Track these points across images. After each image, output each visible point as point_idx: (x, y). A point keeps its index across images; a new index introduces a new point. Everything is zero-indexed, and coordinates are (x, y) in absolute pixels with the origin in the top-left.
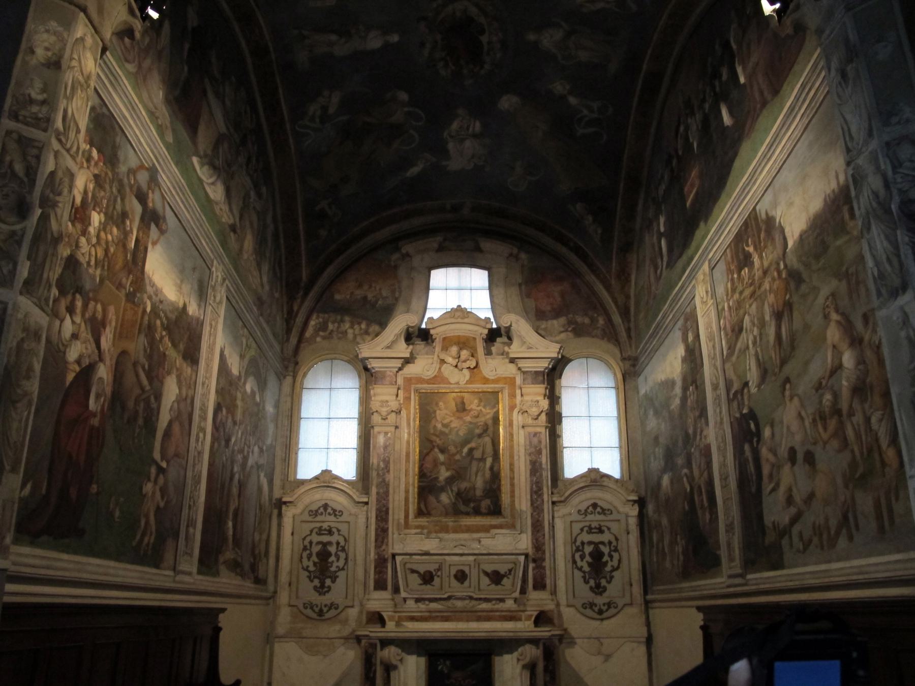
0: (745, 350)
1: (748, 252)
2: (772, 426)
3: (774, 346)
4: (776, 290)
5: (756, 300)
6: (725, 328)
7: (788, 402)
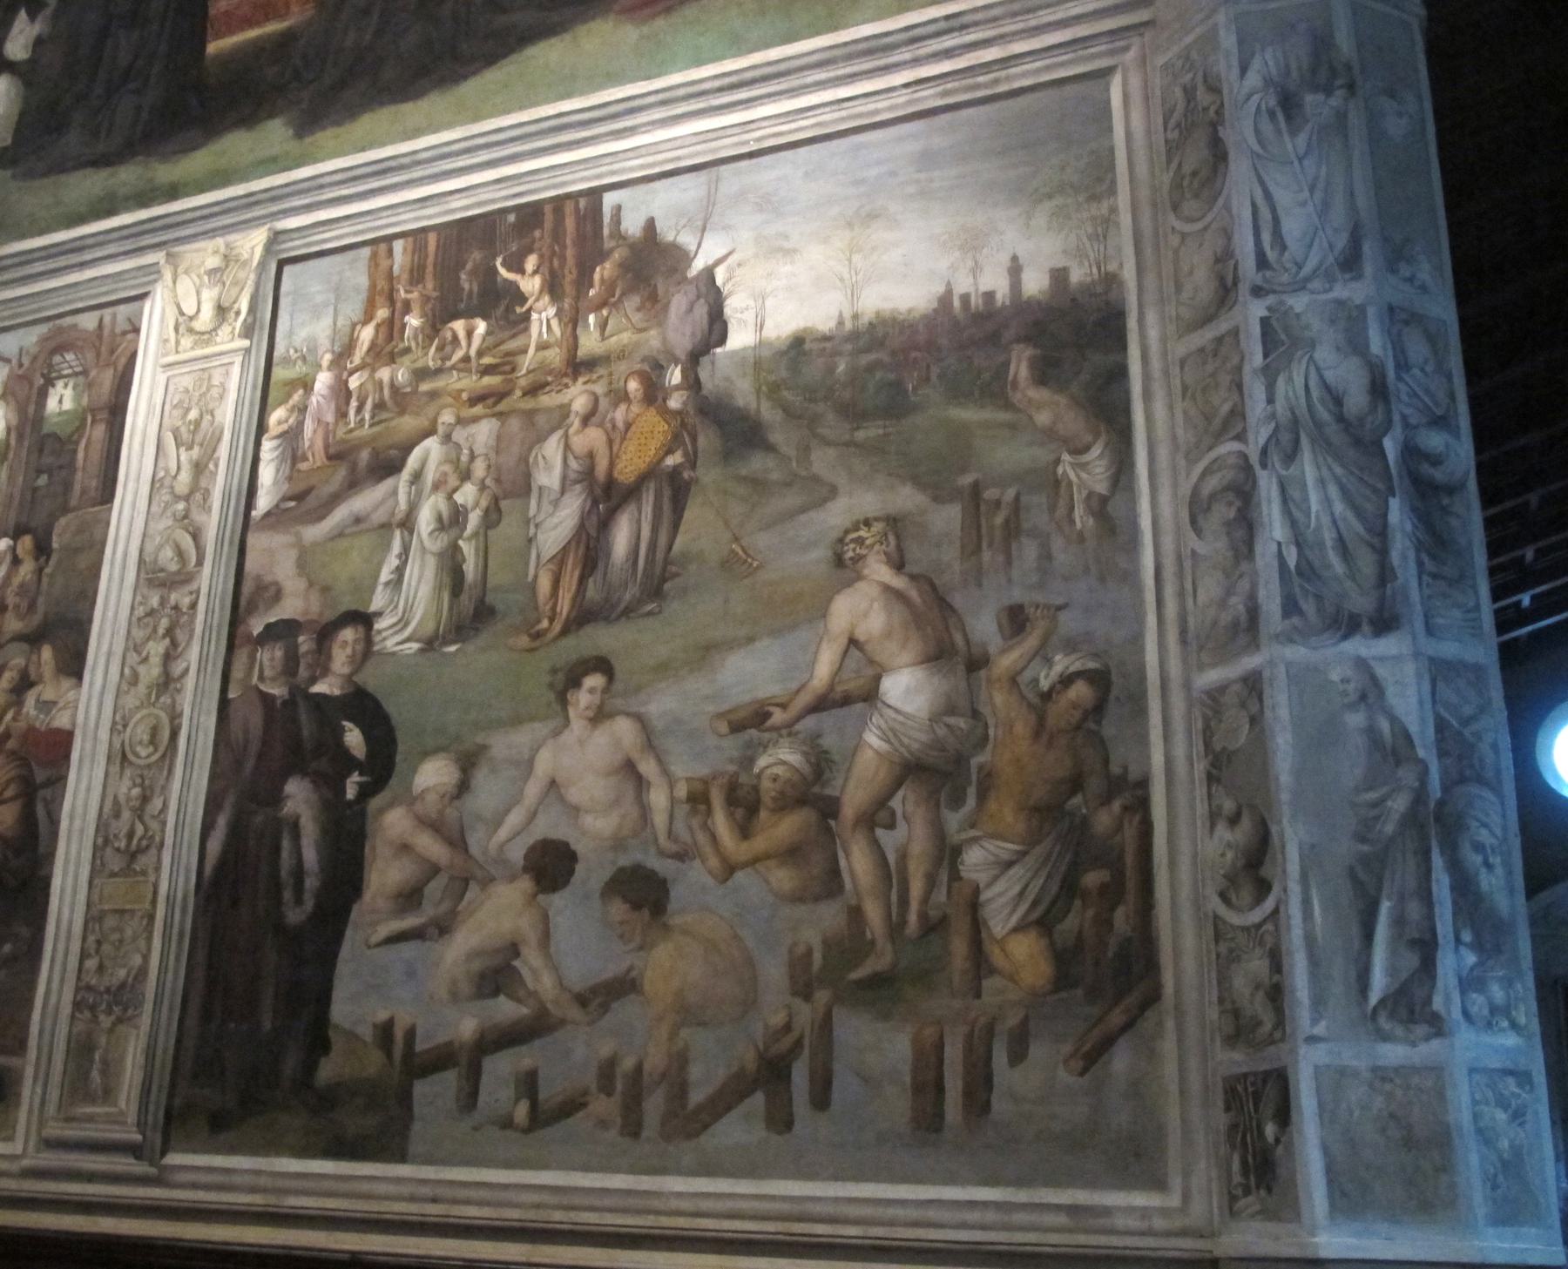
0: (386, 527)
1: (514, 287)
2: (468, 763)
3: (560, 559)
4: (620, 424)
5: (500, 415)
6: (291, 436)
7: (577, 725)
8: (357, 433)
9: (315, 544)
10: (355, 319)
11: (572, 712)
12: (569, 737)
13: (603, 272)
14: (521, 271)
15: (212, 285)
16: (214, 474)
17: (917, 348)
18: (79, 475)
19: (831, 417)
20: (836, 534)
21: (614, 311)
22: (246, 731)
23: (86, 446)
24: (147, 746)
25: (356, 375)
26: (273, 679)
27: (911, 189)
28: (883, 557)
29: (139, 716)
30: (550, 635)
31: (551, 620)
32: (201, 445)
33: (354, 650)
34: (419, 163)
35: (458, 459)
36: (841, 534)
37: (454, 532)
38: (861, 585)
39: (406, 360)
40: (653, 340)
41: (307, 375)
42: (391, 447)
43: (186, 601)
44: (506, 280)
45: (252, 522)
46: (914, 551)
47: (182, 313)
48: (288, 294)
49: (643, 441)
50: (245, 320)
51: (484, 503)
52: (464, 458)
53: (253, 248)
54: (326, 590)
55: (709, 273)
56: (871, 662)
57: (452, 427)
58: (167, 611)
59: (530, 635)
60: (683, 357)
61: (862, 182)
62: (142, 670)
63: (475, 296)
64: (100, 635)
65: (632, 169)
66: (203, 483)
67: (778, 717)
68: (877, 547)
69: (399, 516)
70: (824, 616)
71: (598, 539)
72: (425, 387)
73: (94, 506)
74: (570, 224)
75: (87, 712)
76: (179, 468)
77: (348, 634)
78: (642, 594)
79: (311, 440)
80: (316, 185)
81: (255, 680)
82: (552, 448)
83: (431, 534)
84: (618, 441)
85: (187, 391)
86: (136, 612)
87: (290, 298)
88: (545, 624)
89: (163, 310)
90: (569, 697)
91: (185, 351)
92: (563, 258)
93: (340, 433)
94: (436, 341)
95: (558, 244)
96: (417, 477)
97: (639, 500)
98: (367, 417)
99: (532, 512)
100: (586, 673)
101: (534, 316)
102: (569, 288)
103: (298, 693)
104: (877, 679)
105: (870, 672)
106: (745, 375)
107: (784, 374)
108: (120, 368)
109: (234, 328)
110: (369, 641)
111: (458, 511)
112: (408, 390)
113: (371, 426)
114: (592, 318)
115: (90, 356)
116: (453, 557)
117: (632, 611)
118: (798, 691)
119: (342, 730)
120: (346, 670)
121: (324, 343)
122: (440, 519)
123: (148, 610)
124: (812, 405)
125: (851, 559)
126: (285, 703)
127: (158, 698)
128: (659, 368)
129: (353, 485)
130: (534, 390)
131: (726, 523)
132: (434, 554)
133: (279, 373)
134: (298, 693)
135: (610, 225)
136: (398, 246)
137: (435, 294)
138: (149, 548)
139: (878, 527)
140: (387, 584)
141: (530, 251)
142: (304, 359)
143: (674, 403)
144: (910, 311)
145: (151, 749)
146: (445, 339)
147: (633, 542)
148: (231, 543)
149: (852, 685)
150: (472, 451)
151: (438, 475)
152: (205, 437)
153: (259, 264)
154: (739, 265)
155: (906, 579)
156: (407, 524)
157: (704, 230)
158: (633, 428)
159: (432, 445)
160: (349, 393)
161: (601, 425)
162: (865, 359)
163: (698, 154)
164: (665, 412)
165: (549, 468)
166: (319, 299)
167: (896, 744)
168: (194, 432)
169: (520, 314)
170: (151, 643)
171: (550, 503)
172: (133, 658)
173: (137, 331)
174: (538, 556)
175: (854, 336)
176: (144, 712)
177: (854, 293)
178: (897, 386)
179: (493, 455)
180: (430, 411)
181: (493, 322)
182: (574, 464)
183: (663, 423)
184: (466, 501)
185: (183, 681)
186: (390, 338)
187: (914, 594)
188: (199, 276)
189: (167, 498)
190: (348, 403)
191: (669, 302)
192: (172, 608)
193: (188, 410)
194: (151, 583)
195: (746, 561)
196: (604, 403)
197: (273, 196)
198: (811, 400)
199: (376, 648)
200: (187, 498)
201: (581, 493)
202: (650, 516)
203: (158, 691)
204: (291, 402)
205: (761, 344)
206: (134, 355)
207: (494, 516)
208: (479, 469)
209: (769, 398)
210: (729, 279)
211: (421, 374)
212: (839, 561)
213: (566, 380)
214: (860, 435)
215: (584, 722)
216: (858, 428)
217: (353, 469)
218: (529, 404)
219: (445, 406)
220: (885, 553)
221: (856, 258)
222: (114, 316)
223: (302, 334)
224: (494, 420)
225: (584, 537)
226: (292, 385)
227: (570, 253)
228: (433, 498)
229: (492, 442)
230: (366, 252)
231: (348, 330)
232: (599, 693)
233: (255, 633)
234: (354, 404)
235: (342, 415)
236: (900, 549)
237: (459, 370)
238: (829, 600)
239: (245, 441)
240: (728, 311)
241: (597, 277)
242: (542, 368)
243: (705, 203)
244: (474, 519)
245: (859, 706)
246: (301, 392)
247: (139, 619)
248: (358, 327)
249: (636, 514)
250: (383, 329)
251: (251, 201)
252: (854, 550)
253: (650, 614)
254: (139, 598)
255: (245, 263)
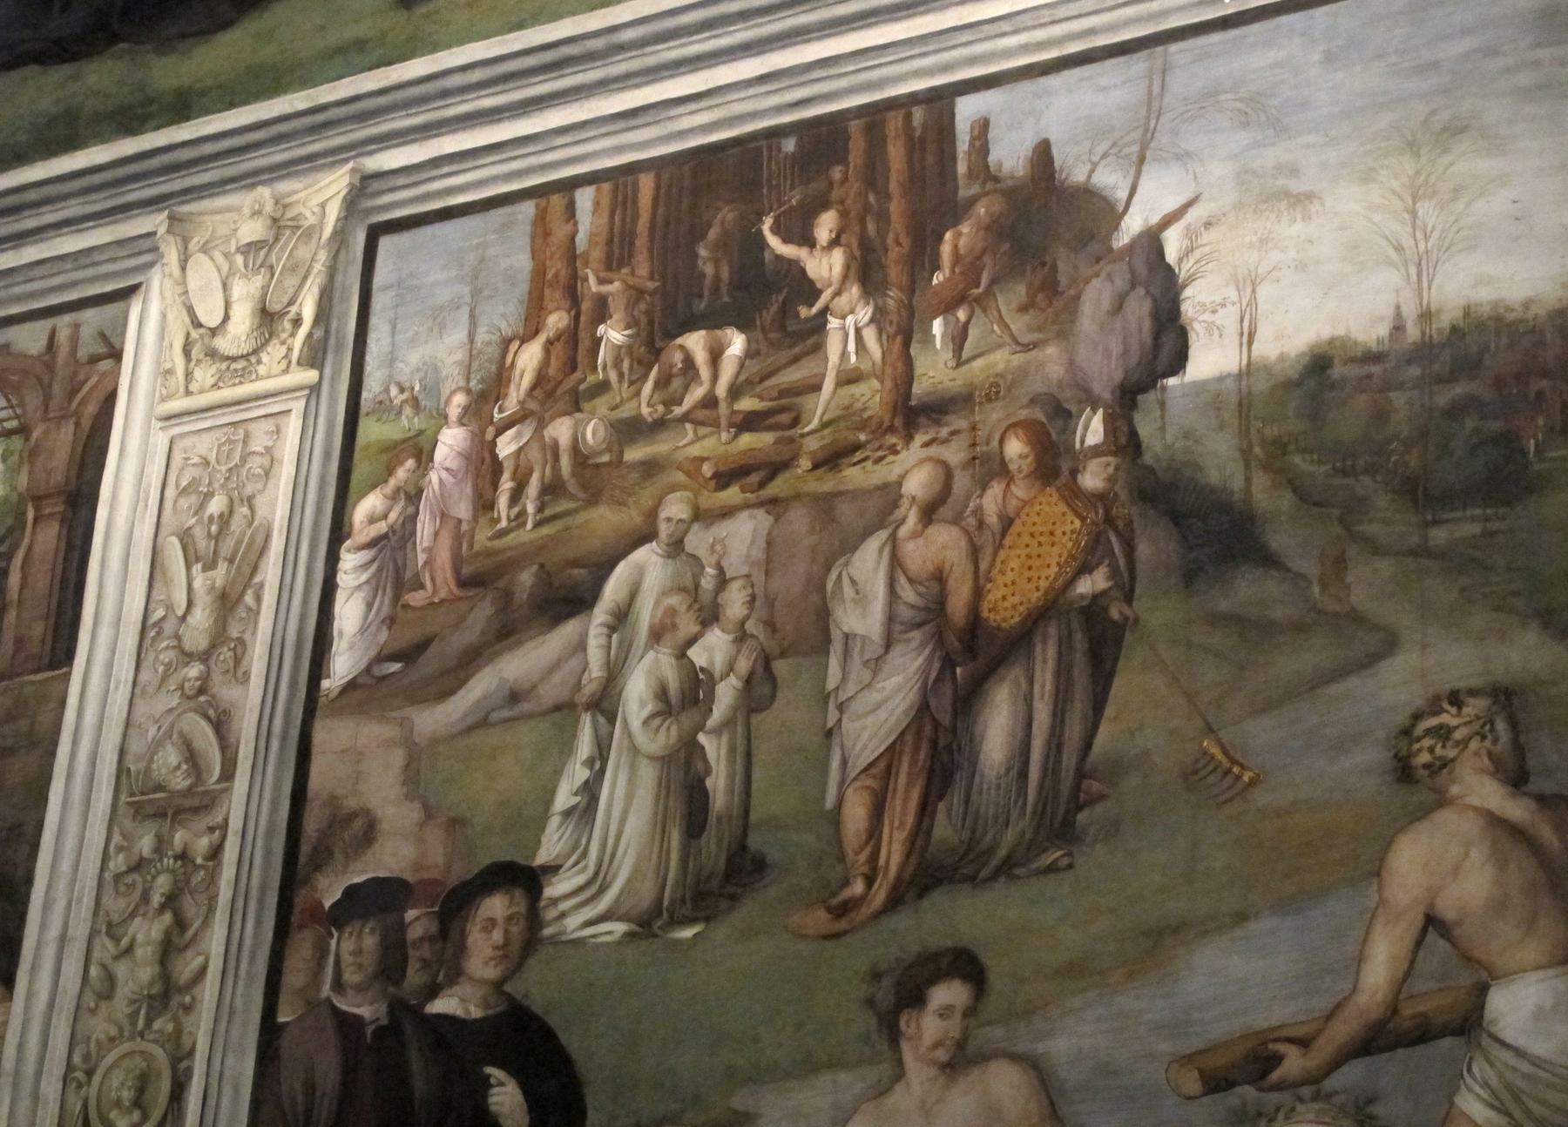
0: (565, 709)
1: (795, 270)
4: (992, 519)
5: (774, 505)
7: (918, 1074)
8: (509, 539)
9: (435, 741)
10: (508, 331)
11: (907, 1049)
12: (900, 1099)
13: (957, 240)
14: (809, 241)
15: (251, 270)
16: (255, 613)
17: (1545, 374)
18: (11, 616)
19: (1382, 501)
20: (1402, 719)
21: (978, 311)
22: (310, 1087)
23: (24, 562)
24: (129, 1112)
25: (511, 433)
26: (360, 988)
27: (1524, 79)
28: (1486, 761)
29: (110, 1059)
30: (866, 911)
31: (870, 881)
32: (231, 561)
33: (506, 932)
34: (622, 48)
35: (697, 586)
36: (1407, 723)
37: (688, 719)
38: (1446, 816)
39: (602, 404)
40: (1052, 362)
41: (421, 432)
42: (576, 563)
43: (203, 843)
44: (779, 258)
45: (322, 700)
46: (1545, 751)
47: (197, 324)
48: (385, 288)
49: (1034, 550)
50: (310, 335)
51: (744, 665)
52: (708, 582)
53: (323, 205)
54: (456, 824)
55: (1152, 240)
56: (1468, 960)
57: (685, 526)
58: (169, 862)
59: (829, 910)
60: (1107, 395)
61: (1435, 65)
62: (121, 970)
63: (724, 289)
64: (47, 906)
65: (1007, 53)
66: (234, 632)
67: (1294, 1063)
68: (1474, 744)
69: (589, 689)
70: (1378, 874)
71: (954, 730)
72: (633, 454)
73: (38, 671)
74: (896, 153)
75: (21, 1047)
76: (190, 604)
77: (496, 906)
78: (1037, 829)
79: (429, 550)
80: (435, 89)
81: (326, 990)
82: (868, 563)
83: (646, 722)
84: (988, 551)
85: (207, 463)
86: (112, 865)
87: (391, 293)
88: (858, 887)
89: (164, 316)
90: (902, 1024)
91: (201, 392)
92: (883, 217)
93: (482, 537)
94: (656, 369)
95: (876, 192)
96: (622, 617)
97: (1030, 656)
98: (530, 508)
99: (832, 683)
100: (933, 980)
101: (833, 323)
102: (895, 273)
103: (405, 1012)
104: (1482, 990)
105: (1466, 979)
106: (1222, 427)
107: (1294, 425)
108: (86, 423)
109: (290, 349)
110: (534, 919)
111: (698, 681)
112: (605, 458)
113: (538, 525)
114: (937, 326)
115: (33, 400)
116: (688, 764)
117: (1018, 865)
118: (1329, 1017)
119: (486, 1083)
120: (491, 973)
121: (452, 376)
122: (662, 694)
123: (135, 858)
124: (1350, 481)
125: (1426, 766)
126: (381, 1033)
127: (149, 1022)
128: (1063, 414)
129: (506, 633)
130: (832, 459)
131: (1190, 697)
132: (652, 758)
133: (371, 431)
134: (405, 1012)
135: (969, 153)
136: (585, 198)
137: (651, 285)
138: (136, 746)
139: (1475, 707)
140: (567, 814)
141: (825, 206)
142: (415, 403)
143: (1092, 479)
144: (1527, 305)
145: (136, 1115)
146: (671, 366)
147: (1020, 736)
148: (284, 738)
149: (1430, 1001)
150: (720, 569)
151: (659, 614)
152: (239, 542)
153: (335, 233)
154: (1208, 225)
155: (1533, 805)
156: (605, 703)
157: (1142, 160)
158: (1016, 527)
159: (648, 562)
160: (497, 467)
161: (956, 521)
162: (1444, 397)
163: (1126, 23)
164: (1073, 493)
165: (861, 598)
166: (444, 296)
167: (1518, 1114)
168: (217, 538)
169: (808, 320)
170: (138, 920)
171: (866, 663)
172: (105, 948)
173: (117, 355)
174: (844, 763)
175: (1424, 351)
176: (125, 1047)
177: (1422, 268)
178: (1508, 442)
179: (759, 578)
180: (646, 497)
181: (758, 334)
182: (908, 593)
183: (1070, 516)
184: (712, 663)
185: (196, 990)
186: (571, 365)
187: (1547, 835)
188: (226, 255)
189: (168, 656)
190: (495, 485)
191: (1077, 298)
192: (176, 858)
193: (209, 495)
194: (138, 810)
195: (1228, 772)
196: (961, 482)
197: (360, 111)
198: (1344, 473)
199: (548, 932)
200: (205, 657)
201: (923, 645)
202: (1049, 687)
203: (150, 1007)
204: (393, 482)
205: (1249, 371)
206: (111, 398)
207: (765, 690)
208: (735, 603)
209: (1266, 468)
210: (1189, 251)
211: (630, 430)
212: (1404, 772)
213: (892, 439)
214: (1439, 536)
215: (933, 1071)
216: (1436, 523)
217: (507, 596)
218: (827, 484)
219: (673, 488)
220: (1490, 754)
221: (1425, 209)
222: (77, 326)
223: (412, 360)
224: (760, 513)
225: (928, 729)
226: (394, 452)
227: (896, 208)
228: (651, 655)
229: (758, 553)
230: (528, 209)
231: (494, 351)
232: (958, 1016)
233: (327, 904)
234: (506, 484)
235: (485, 505)
236: (1518, 749)
237: (698, 423)
238: (1389, 844)
239: (309, 553)
240: (1187, 309)
241: (946, 249)
242: (847, 416)
243: (1143, 112)
244: (726, 694)
245: (1447, 1042)
246: (410, 463)
247: (118, 877)
248: (514, 346)
249: (1023, 680)
250: (558, 349)
251: (319, 121)
252: (1431, 750)
253: (1052, 869)
254: (117, 838)
255: (309, 233)
